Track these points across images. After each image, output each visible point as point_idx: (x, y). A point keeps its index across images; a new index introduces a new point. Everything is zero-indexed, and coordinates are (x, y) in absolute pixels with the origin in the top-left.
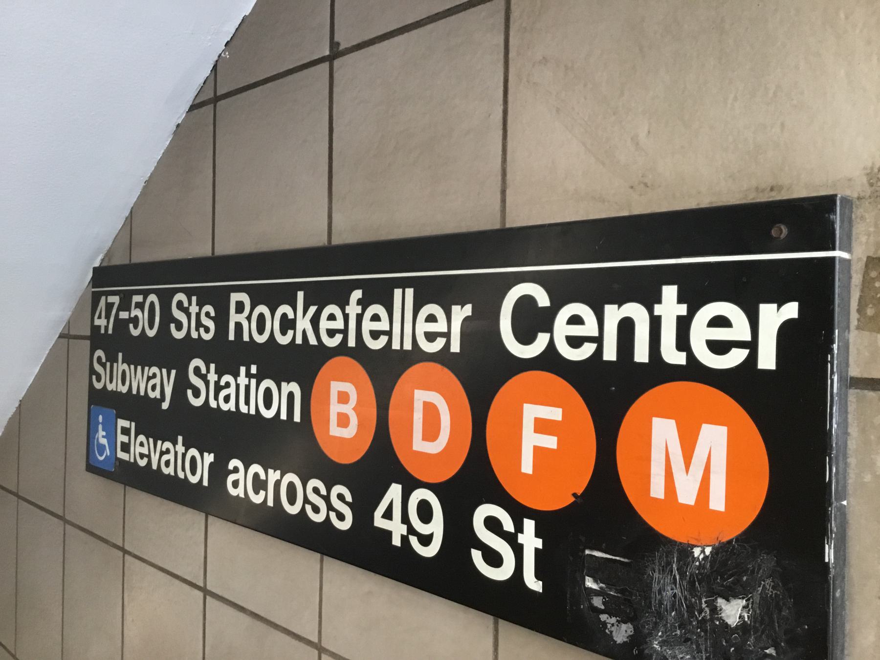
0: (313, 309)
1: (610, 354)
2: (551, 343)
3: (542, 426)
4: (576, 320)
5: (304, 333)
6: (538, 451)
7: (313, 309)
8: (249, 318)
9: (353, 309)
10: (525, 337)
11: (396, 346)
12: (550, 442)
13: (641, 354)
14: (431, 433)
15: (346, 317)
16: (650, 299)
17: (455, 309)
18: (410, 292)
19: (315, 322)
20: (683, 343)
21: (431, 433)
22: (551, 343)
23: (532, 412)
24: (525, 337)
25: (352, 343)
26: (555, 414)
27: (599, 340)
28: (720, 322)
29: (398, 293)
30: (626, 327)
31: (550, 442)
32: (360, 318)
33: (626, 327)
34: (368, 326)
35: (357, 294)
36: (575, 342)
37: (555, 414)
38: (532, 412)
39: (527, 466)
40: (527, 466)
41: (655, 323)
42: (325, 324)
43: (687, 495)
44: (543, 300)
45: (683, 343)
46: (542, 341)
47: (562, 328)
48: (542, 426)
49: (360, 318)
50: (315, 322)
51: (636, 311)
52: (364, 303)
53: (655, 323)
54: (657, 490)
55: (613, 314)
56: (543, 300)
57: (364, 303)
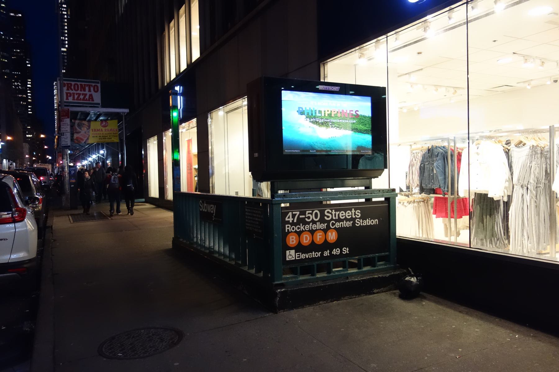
0: (304, 226)
1: (340, 227)
2: (335, 227)
3: (320, 235)
4: (337, 224)
5: (302, 229)
6: (320, 238)
7: (304, 226)
8: (290, 228)
9: (311, 225)
10: (333, 226)
11: (317, 229)
12: (321, 237)
13: (343, 226)
14: (306, 239)
15: (310, 226)
16: (343, 222)
17: (325, 224)
18: (319, 223)
19: (304, 227)
20: (346, 225)
21: (306, 239)
22: (335, 227)
23: (318, 234)
24: (333, 226)
25: (311, 229)
26: (321, 234)
27: (350, 225)
28: (348, 223)
29: (317, 223)
30: (342, 224)
31: (321, 237)
32: (312, 226)
33: (342, 224)
34: (313, 227)
35: (311, 223)
36: (337, 226)
37: (321, 234)
38: (318, 234)
39: (318, 240)
40: (318, 240)
41: (344, 224)
42: (306, 227)
43: (332, 239)
44: (334, 222)
45: (346, 225)
46: (334, 226)
47: (336, 225)
48: (320, 235)
49: (312, 226)
50: (304, 227)
51: (342, 223)
52: (312, 224)
53: (344, 224)
54: (329, 239)
55: (341, 223)
56: (334, 222)
57: (312, 224)
